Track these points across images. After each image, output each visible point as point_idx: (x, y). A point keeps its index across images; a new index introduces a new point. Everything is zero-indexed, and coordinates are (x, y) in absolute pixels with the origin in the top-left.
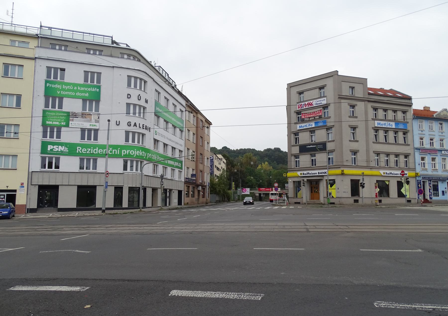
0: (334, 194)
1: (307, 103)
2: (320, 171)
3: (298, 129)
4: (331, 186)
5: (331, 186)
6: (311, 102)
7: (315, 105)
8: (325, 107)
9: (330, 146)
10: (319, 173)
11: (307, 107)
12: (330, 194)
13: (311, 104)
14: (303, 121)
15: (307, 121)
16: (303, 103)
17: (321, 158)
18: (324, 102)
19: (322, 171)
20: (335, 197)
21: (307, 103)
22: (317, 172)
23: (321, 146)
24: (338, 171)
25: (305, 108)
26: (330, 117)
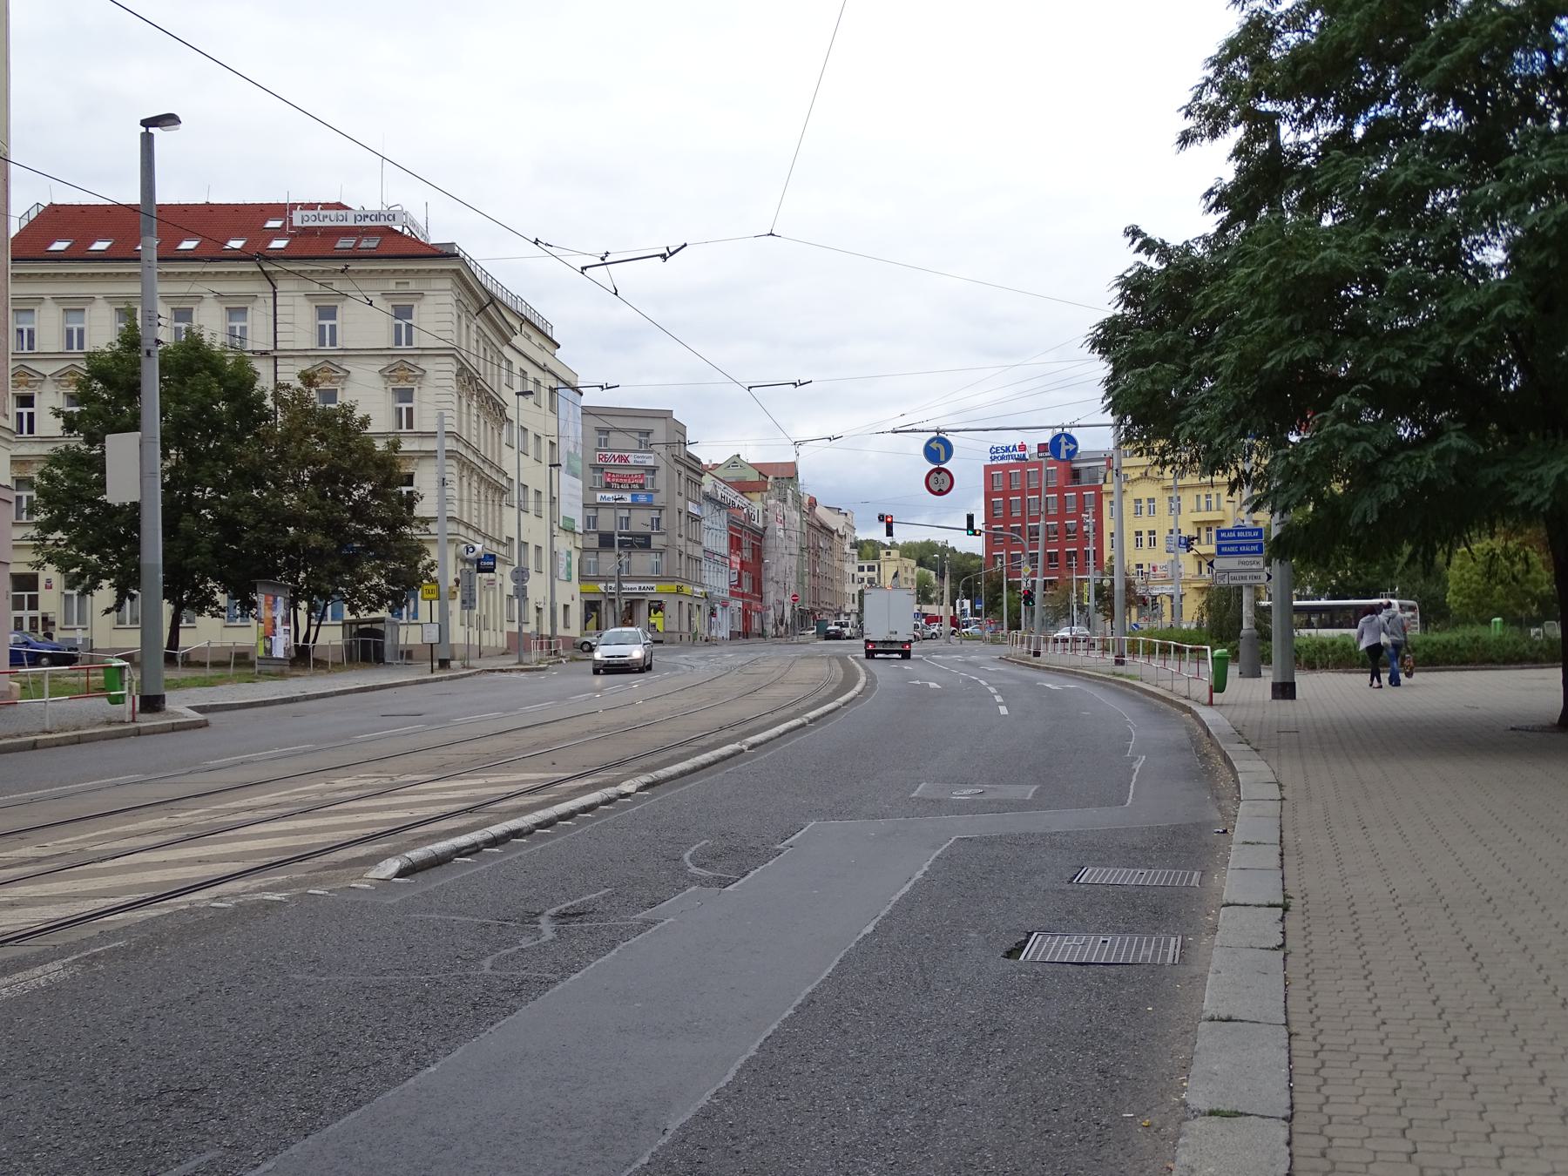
0: (660, 627)
1: (617, 454)
2: (642, 585)
3: (598, 500)
4: (655, 613)
5: (655, 613)
6: (627, 455)
7: (632, 463)
8: (653, 470)
9: (656, 541)
10: (640, 588)
11: (617, 462)
12: (654, 625)
13: (626, 460)
14: (608, 487)
15: (615, 490)
16: (609, 454)
17: (641, 562)
18: (650, 462)
19: (646, 585)
20: (661, 630)
21: (617, 454)
22: (636, 585)
23: (641, 540)
24: (673, 587)
25: (612, 463)
26: (658, 491)
